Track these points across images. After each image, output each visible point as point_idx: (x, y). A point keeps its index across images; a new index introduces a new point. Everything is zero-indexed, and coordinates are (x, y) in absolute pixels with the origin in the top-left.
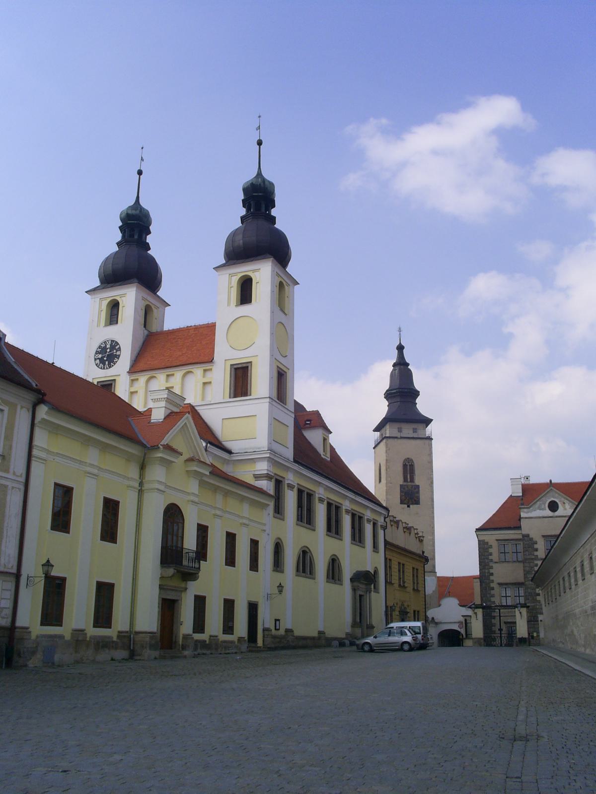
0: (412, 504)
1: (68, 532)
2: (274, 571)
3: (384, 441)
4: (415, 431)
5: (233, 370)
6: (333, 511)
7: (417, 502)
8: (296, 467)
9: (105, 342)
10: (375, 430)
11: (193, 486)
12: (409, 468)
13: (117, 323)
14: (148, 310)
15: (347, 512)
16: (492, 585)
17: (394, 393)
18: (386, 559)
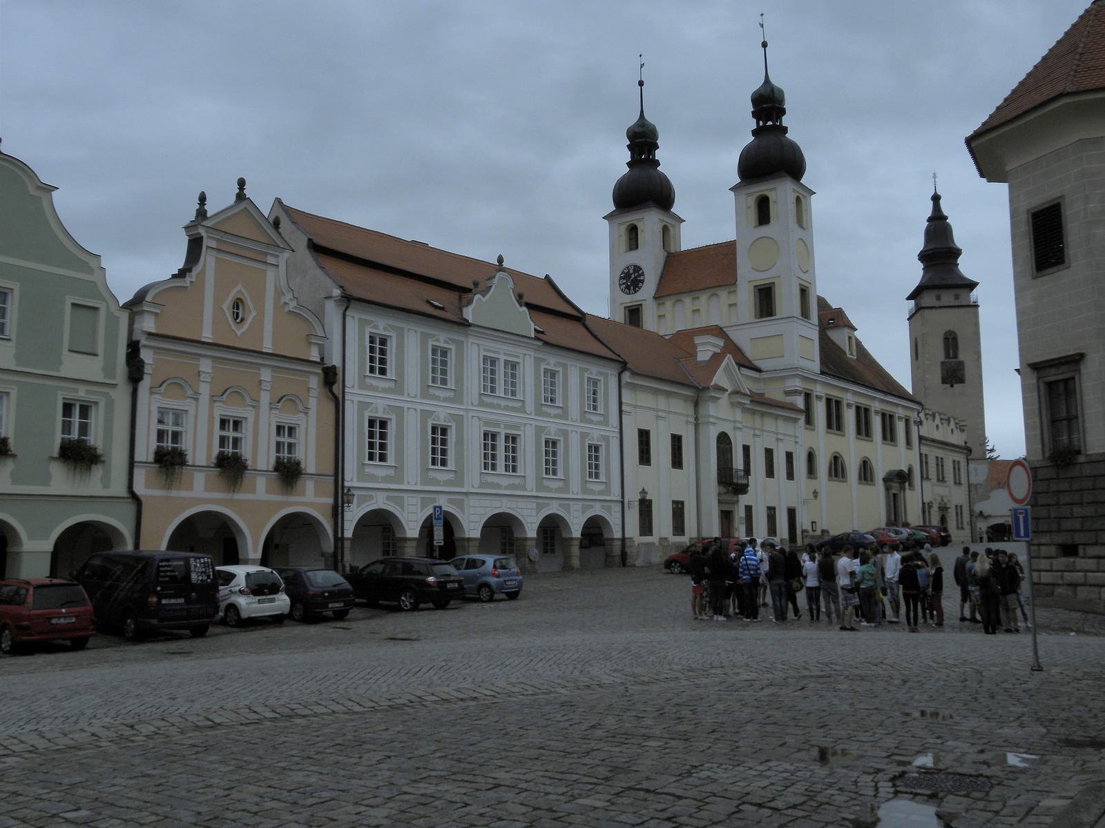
0: (956, 383)
1: (650, 465)
2: (808, 478)
4: (957, 297)
5: (757, 294)
6: (863, 415)
7: (962, 381)
8: (823, 378)
9: (628, 268)
10: (909, 298)
11: (739, 415)
12: (951, 341)
13: (637, 248)
14: (665, 230)
15: (876, 412)
18: (921, 454)
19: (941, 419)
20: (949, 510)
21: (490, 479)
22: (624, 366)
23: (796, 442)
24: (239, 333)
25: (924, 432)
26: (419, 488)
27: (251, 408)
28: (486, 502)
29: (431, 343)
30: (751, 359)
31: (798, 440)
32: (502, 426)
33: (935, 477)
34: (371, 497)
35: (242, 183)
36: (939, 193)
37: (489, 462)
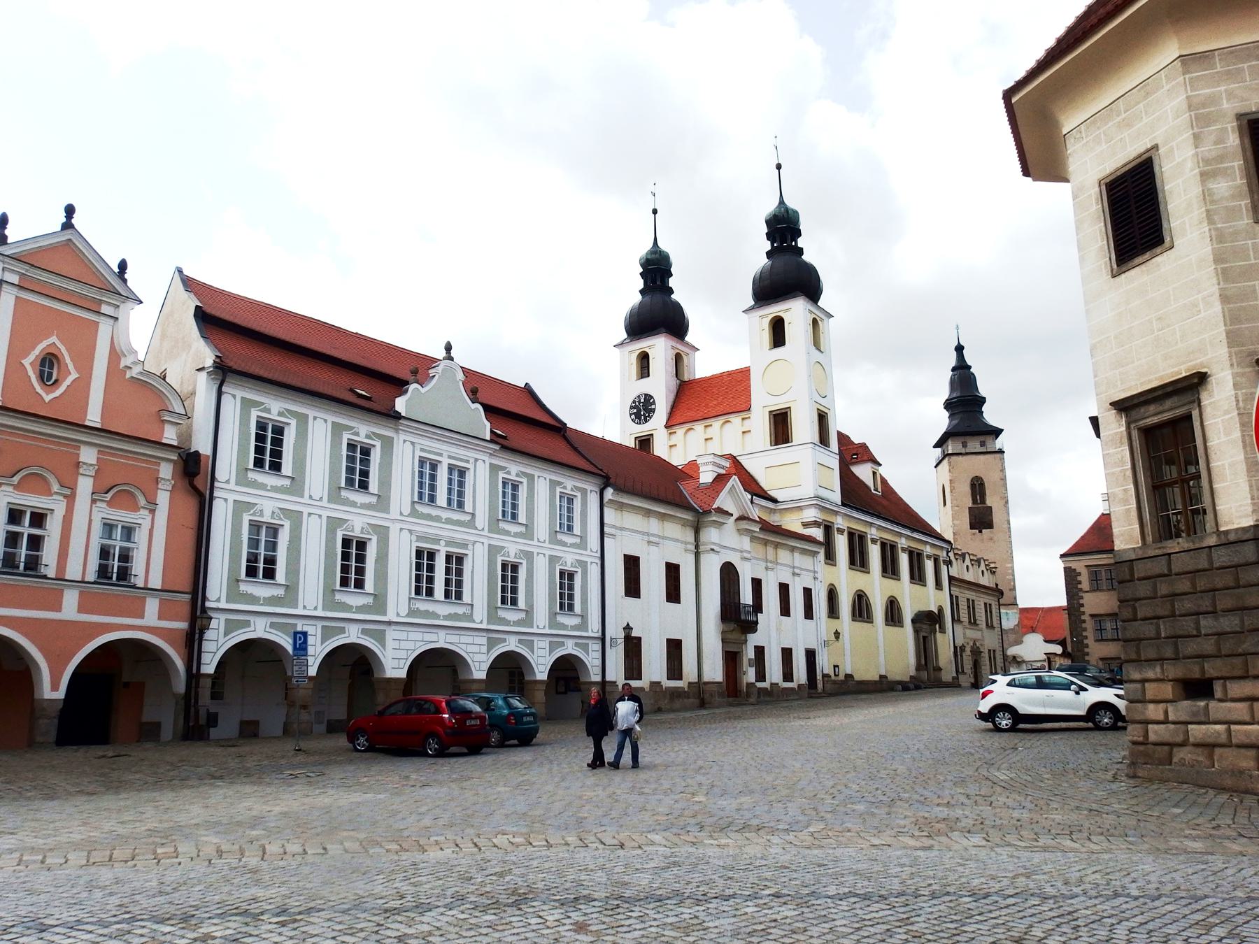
2: (829, 617)
3: (947, 459)
4: (983, 444)
8: (845, 510)
10: (935, 447)
11: (746, 543)
12: (978, 487)
13: (649, 376)
14: (678, 358)
15: (903, 550)
16: (1083, 617)
17: (955, 402)
18: (951, 596)
19: (971, 560)
20: (983, 654)
21: (423, 606)
22: (606, 482)
23: (815, 578)
24: (47, 398)
25: (954, 573)
26: (320, 613)
27: (61, 498)
28: (416, 635)
29: (346, 437)
30: (766, 489)
31: (819, 576)
32: (442, 543)
33: (967, 620)
34: (247, 624)
35: (70, 211)
36: (962, 343)
37: (423, 587)
